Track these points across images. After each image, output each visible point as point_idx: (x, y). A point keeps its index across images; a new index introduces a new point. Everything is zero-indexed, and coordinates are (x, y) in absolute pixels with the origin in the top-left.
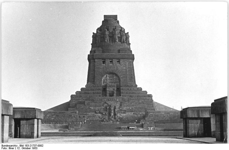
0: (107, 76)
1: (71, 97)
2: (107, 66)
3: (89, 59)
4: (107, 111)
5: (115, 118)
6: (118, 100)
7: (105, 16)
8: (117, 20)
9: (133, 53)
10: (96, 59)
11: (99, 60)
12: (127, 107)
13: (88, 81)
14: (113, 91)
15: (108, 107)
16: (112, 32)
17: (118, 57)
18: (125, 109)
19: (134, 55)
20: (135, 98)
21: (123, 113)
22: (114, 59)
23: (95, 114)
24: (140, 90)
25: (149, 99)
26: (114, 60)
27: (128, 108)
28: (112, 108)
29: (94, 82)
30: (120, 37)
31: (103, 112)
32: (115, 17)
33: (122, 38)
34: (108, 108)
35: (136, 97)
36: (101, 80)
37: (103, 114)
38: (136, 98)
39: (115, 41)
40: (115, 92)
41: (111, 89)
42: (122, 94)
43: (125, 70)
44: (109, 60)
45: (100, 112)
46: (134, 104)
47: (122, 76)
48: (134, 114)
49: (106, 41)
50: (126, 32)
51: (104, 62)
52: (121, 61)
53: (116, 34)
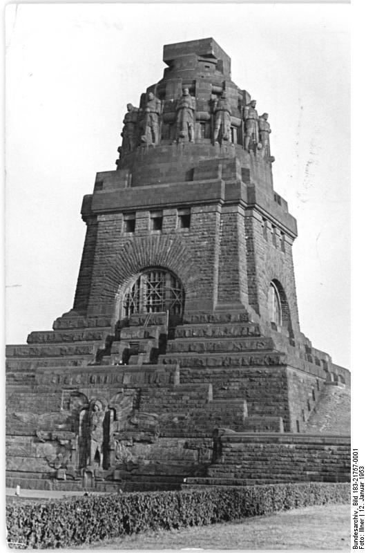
0: (139, 282)
2: (138, 240)
3: (84, 218)
6: (126, 381)
7: (165, 46)
10: (101, 214)
11: (111, 217)
12: (160, 412)
15: (83, 413)
17: (184, 197)
18: (152, 423)
20: (214, 373)
21: (142, 441)
22: (167, 208)
23: (34, 445)
24: (253, 335)
25: (270, 376)
26: (166, 212)
27: (165, 416)
30: (209, 121)
31: (61, 434)
32: (205, 50)
34: (81, 418)
35: (219, 366)
36: (112, 299)
37: (63, 442)
38: (217, 370)
43: (206, 253)
44: (148, 214)
45: (50, 435)
46: (191, 398)
47: (192, 279)
48: (186, 446)
49: (147, 137)
51: (131, 226)
52: (194, 217)
53: (183, 108)
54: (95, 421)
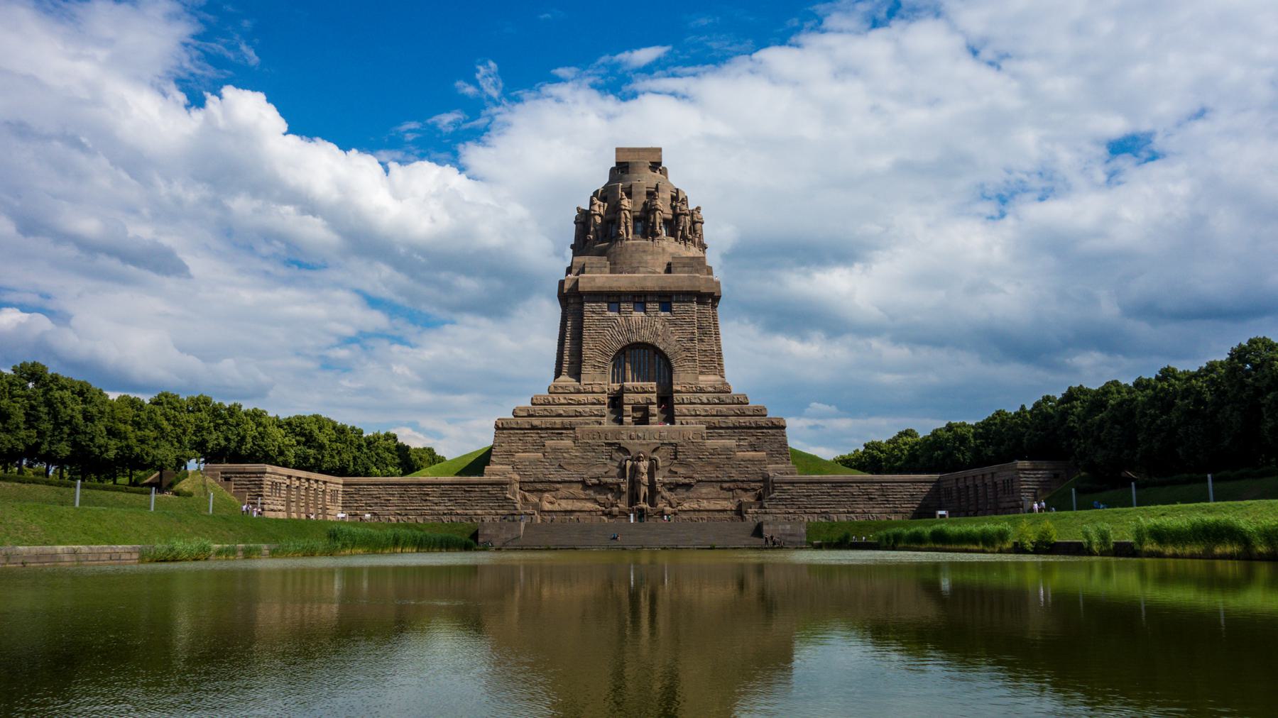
1: (497, 428)
4: (624, 477)
5: (652, 504)
7: (618, 150)
8: (660, 164)
13: (558, 373)
16: (645, 204)
28: (644, 465)
29: (577, 375)
33: (678, 224)
39: (655, 235)
40: (654, 409)
41: (640, 398)
42: (677, 420)
54: (643, 470)
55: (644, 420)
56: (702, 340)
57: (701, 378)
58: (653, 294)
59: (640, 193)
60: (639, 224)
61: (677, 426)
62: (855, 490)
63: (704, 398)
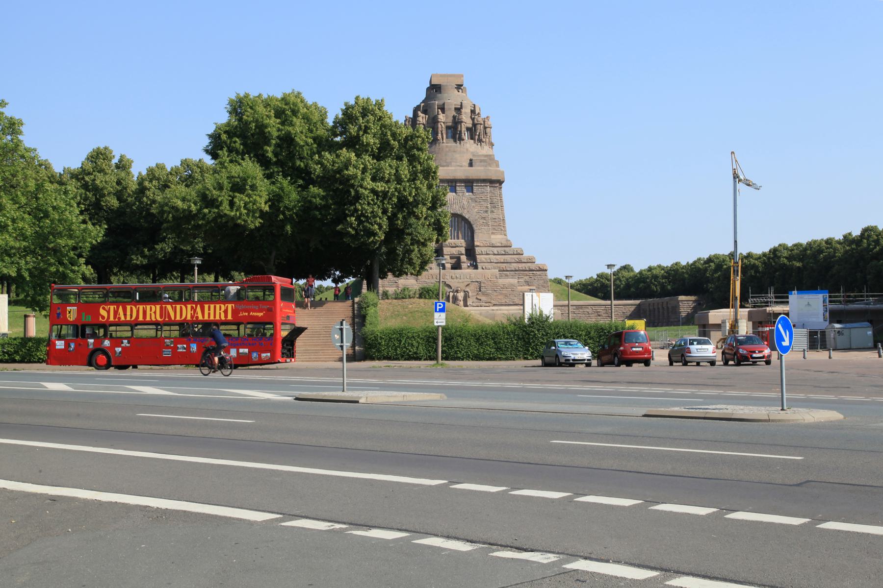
9: (501, 168)
14: (459, 259)
19: (503, 172)
24: (519, 254)
40: (464, 258)
41: (454, 251)
42: (480, 266)
50: (483, 116)
55: (457, 266)
56: (492, 212)
57: (493, 236)
58: (461, 181)
59: (450, 109)
60: (450, 131)
61: (480, 270)
62: (590, 310)
63: (495, 250)
